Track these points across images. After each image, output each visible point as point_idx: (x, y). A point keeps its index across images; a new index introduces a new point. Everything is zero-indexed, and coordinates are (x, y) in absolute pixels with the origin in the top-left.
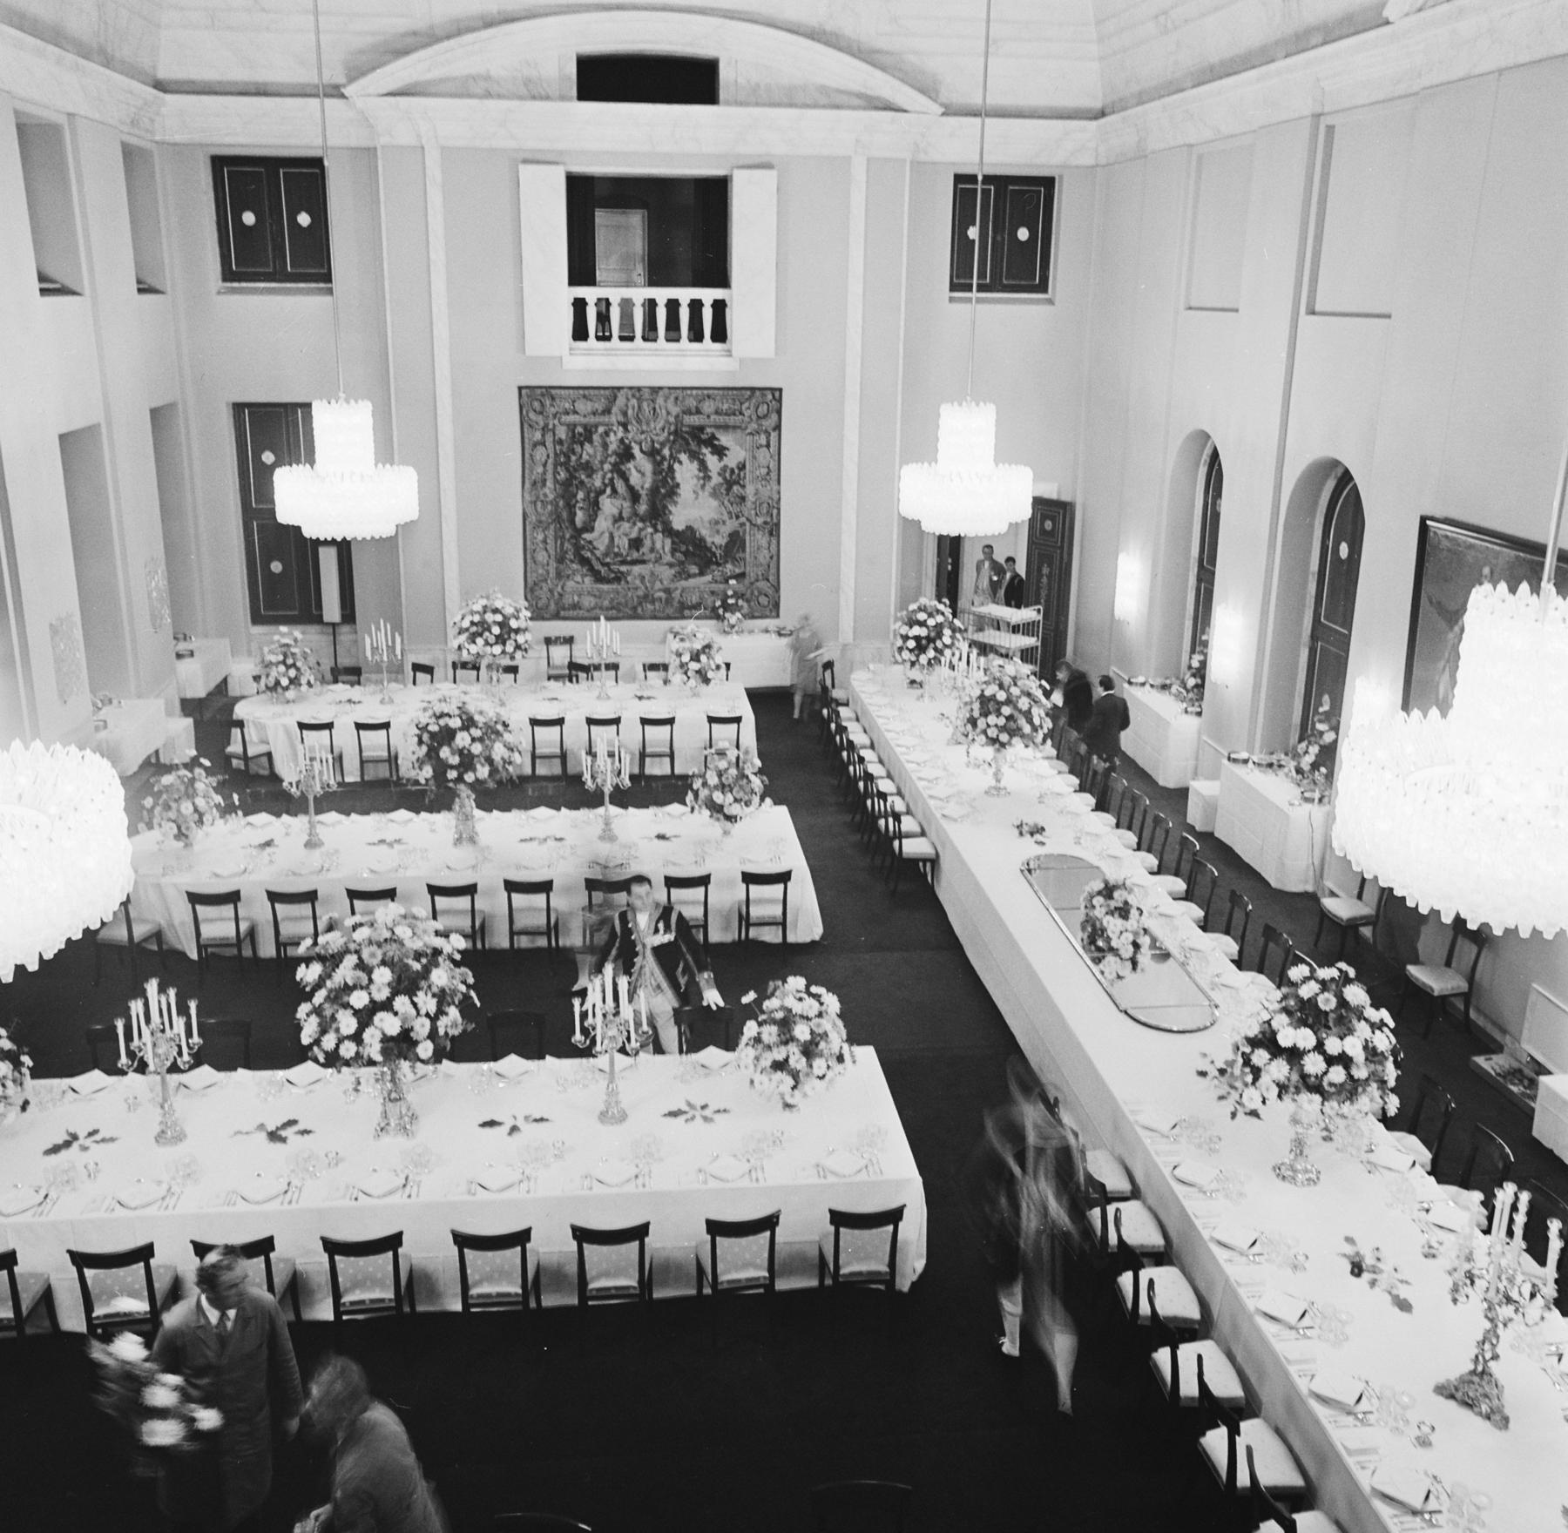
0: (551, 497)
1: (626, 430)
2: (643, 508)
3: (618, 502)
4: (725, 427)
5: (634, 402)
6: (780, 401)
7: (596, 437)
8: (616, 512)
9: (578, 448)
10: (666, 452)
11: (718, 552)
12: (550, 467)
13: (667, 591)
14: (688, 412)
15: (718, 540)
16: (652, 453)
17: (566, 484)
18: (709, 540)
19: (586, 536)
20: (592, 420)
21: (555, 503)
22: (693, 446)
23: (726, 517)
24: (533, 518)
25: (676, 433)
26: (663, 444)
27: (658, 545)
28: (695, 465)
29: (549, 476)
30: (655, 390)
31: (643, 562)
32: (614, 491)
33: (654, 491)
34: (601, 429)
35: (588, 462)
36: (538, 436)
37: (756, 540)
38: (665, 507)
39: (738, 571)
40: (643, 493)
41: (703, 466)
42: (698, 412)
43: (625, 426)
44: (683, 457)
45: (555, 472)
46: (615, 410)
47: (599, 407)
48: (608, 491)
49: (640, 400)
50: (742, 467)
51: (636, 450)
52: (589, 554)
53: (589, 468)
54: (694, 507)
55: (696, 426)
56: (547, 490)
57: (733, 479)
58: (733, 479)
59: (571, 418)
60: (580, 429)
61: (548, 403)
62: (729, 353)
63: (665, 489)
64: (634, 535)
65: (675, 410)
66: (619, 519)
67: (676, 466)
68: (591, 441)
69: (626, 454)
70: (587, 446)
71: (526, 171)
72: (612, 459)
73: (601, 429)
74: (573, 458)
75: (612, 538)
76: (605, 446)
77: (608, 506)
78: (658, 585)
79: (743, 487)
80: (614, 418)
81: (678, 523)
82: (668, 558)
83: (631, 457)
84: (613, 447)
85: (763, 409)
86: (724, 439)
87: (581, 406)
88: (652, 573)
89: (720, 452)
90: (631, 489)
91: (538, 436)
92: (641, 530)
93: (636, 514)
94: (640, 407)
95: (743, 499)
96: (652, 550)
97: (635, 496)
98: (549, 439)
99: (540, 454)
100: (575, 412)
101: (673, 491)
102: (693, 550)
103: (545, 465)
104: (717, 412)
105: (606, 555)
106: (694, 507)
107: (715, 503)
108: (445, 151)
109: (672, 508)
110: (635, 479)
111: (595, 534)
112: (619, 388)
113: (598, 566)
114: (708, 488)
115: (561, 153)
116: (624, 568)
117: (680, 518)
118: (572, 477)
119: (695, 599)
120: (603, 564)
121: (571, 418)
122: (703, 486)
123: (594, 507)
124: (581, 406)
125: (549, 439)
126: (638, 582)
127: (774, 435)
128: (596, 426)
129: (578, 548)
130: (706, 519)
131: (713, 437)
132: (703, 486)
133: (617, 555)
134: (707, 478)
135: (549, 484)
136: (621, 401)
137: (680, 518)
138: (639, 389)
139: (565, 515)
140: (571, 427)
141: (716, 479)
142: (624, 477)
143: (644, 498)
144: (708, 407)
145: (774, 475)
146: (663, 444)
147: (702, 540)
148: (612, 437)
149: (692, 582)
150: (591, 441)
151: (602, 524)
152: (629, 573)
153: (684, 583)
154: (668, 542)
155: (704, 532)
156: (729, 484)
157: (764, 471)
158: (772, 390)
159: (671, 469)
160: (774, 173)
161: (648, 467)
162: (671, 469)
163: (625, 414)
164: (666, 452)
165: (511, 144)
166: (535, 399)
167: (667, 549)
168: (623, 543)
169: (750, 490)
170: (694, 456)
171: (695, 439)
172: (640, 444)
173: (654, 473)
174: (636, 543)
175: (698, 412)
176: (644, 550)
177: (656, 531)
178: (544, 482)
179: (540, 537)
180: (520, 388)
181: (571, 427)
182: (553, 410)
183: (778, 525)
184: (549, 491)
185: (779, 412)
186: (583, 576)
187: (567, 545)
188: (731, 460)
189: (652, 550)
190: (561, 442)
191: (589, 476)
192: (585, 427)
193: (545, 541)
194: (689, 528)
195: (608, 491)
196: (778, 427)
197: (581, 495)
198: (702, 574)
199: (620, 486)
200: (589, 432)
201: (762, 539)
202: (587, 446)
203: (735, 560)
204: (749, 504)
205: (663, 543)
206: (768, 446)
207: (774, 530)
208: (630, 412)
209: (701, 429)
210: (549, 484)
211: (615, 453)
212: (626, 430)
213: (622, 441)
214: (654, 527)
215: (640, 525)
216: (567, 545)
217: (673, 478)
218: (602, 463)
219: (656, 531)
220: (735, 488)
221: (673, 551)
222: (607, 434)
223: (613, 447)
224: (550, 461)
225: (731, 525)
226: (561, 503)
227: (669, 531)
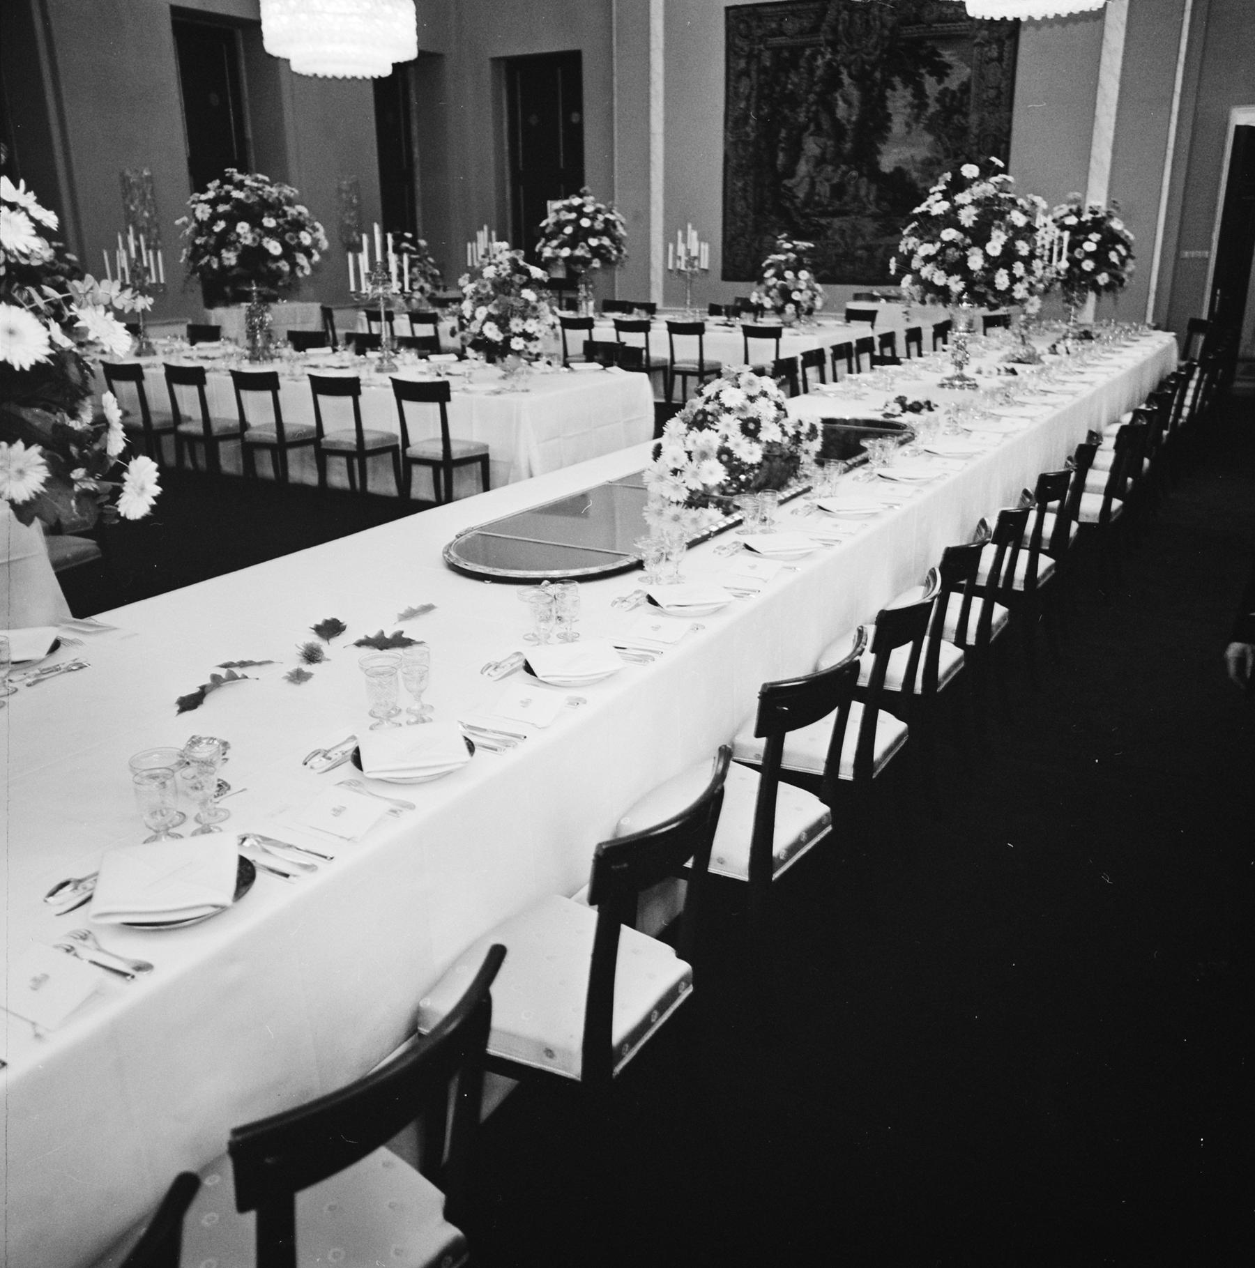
0: (753, 135)
1: (835, 52)
5: (845, 14)
7: (802, 63)
8: (817, 151)
12: (753, 100)
16: (861, 79)
19: (786, 182)
20: (799, 40)
23: (941, 157)
24: (733, 162)
26: (874, 66)
27: (863, 192)
31: (846, 213)
32: (819, 126)
33: (861, 124)
34: (808, 52)
35: (792, 92)
36: (742, 64)
41: (920, 93)
42: (918, 20)
43: (833, 44)
44: (897, 80)
45: (759, 108)
46: (824, 27)
48: (812, 127)
50: (965, 88)
53: (793, 101)
56: (748, 129)
57: (954, 104)
60: (786, 54)
61: (754, 24)
63: (874, 125)
66: (820, 161)
67: (889, 93)
69: (833, 82)
72: (817, 89)
73: (808, 52)
74: (778, 89)
76: (811, 71)
77: (812, 147)
79: (966, 115)
82: (872, 209)
83: (840, 84)
84: (819, 72)
86: (948, 56)
88: (854, 227)
90: (835, 122)
92: (845, 173)
94: (851, 21)
95: (964, 130)
97: (838, 131)
100: (782, 34)
105: (806, 203)
107: (929, 138)
109: (883, 148)
110: (841, 110)
111: (797, 179)
113: (797, 219)
114: (924, 120)
116: (823, 221)
125: (754, 67)
126: (837, 237)
127: (1008, 43)
128: (803, 48)
130: (918, 158)
132: (917, 119)
133: (819, 204)
140: (776, 51)
142: (831, 109)
146: (874, 66)
148: (820, 62)
150: (796, 67)
151: (803, 168)
154: (874, 187)
155: (915, 175)
157: (992, 93)
159: (883, 99)
161: (855, 94)
163: (834, 30)
164: (878, 75)
167: (872, 198)
168: (824, 189)
169: (974, 119)
172: (848, 66)
175: (918, 20)
176: (846, 198)
177: (861, 175)
179: (740, 184)
181: (776, 51)
182: (760, 32)
188: (953, 83)
189: (856, 198)
191: (793, 110)
193: (744, 190)
195: (812, 127)
197: (783, 134)
204: (972, 139)
205: (867, 190)
208: (840, 28)
213: (828, 65)
214: (858, 169)
215: (844, 167)
217: (885, 108)
218: (808, 92)
219: (861, 175)
222: (813, 57)
223: (819, 72)
224: (754, 93)
226: (763, 145)
227: (875, 174)
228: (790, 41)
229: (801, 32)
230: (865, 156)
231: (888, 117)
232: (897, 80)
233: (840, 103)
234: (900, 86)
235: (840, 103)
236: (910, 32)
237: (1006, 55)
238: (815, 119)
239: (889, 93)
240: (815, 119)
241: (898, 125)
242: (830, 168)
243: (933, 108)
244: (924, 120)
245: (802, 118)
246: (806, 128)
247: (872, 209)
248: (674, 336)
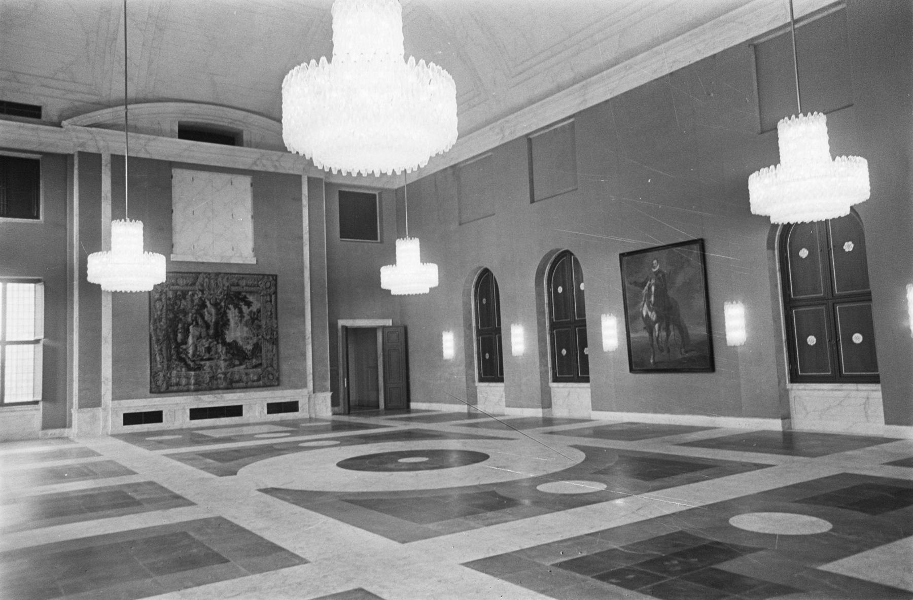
1: (203, 293)
2: (211, 332)
3: (199, 329)
4: (251, 293)
5: (206, 280)
6: (276, 280)
7: (188, 297)
8: (197, 333)
9: (178, 302)
10: (223, 304)
11: (249, 353)
12: (164, 311)
13: (225, 374)
14: (233, 285)
16: (216, 305)
19: (184, 347)
26: (221, 300)
27: (220, 350)
30: (218, 274)
32: (197, 323)
33: (217, 323)
37: (266, 347)
38: (222, 331)
40: (212, 324)
41: (241, 311)
42: (238, 285)
43: (202, 291)
44: (231, 306)
46: (197, 283)
47: (190, 281)
50: (259, 311)
51: (208, 303)
54: (236, 332)
57: (255, 317)
63: (222, 323)
65: (227, 284)
66: (199, 337)
68: (185, 298)
69: (203, 305)
70: (183, 301)
76: (192, 301)
78: (219, 371)
81: (228, 340)
83: (206, 306)
84: (196, 302)
86: (251, 298)
89: (249, 304)
90: (206, 322)
93: (208, 335)
95: (260, 327)
101: (226, 323)
102: (236, 352)
106: (236, 332)
107: (246, 329)
112: (200, 273)
114: (243, 322)
116: (202, 363)
117: (230, 337)
118: (175, 317)
119: (237, 377)
120: (193, 361)
121: (176, 287)
122: (241, 321)
123: (186, 332)
124: (180, 282)
125: (163, 297)
128: (188, 291)
129: (178, 353)
131: (245, 297)
132: (241, 321)
133: (199, 356)
137: (230, 337)
138: (209, 274)
139: (172, 336)
140: (175, 292)
141: (247, 317)
142: (203, 317)
145: (274, 315)
146: (221, 300)
147: (241, 347)
148: (196, 297)
149: (236, 369)
150: (185, 298)
152: (205, 365)
153: (231, 370)
155: (241, 343)
156: (253, 320)
158: (273, 276)
159: (225, 313)
161: (213, 311)
163: (202, 285)
164: (223, 304)
168: (202, 350)
169: (263, 322)
170: (236, 306)
171: (237, 298)
172: (210, 300)
173: (217, 314)
174: (209, 350)
175: (238, 285)
176: (212, 353)
181: (175, 292)
185: (276, 285)
186: (181, 367)
187: (173, 352)
188: (254, 308)
189: (217, 353)
190: (170, 299)
192: (182, 292)
194: (235, 341)
196: (275, 293)
197: (180, 326)
198: (241, 364)
202: (183, 301)
203: (257, 357)
206: (271, 301)
207: (275, 341)
209: (240, 293)
212: (203, 293)
213: (200, 298)
216: (173, 352)
221: (227, 353)
222: (193, 295)
223: (196, 302)
225: (255, 340)
227: (224, 343)
229: (187, 285)
231: (228, 320)
232: (231, 306)
234: (233, 309)
236: (233, 289)
238: (195, 320)
240: (195, 320)
244: (243, 322)
245: (189, 320)
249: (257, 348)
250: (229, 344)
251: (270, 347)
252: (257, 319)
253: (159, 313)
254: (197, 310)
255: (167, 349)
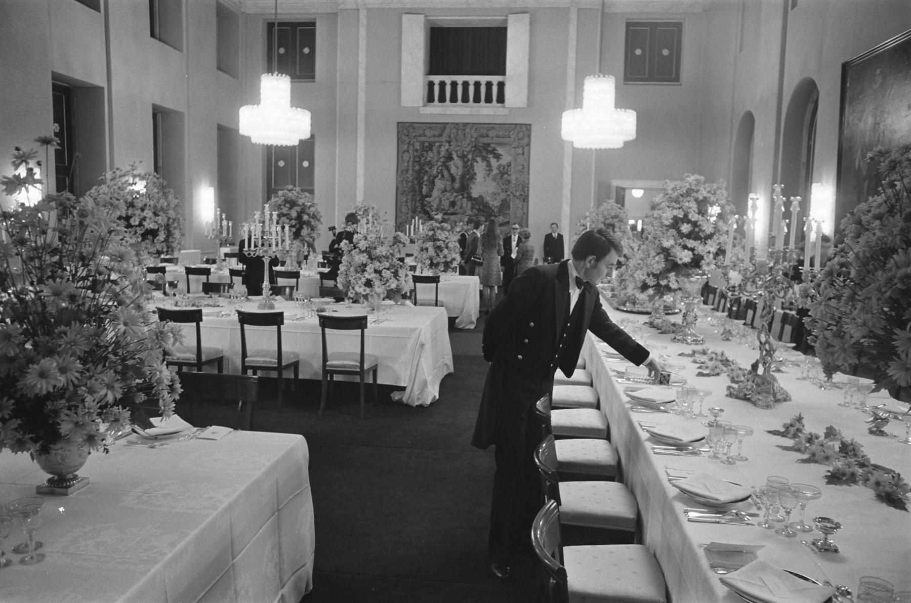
0: (411, 178)
1: (450, 145)
2: (457, 185)
3: (445, 182)
4: (501, 144)
5: (454, 131)
6: (530, 130)
7: (434, 148)
8: (443, 187)
9: (425, 154)
10: (470, 156)
11: (496, 210)
12: (411, 163)
15: (495, 203)
16: (463, 157)
17: (419, 172)
18: (491, 203)
20: (433, 139)
21: (412, 182)
22: (484, 154)
23: (500, 191)
24: (401, 189)
25: (475, 146)
26: (468, 153)
27: (464, 205)
28: (485, 163)
29: (410, 168)
31: (456, 214)
32: (443, 176)
33: (463, 177)
34: (437, 144)
36: (405, 147)
37: (515, 204)
39: (506, 220)
40: (457, 177)
41: (489, 165)
42: (487, 136)
43: (449, 142)
44: (479, 159)
45: (414, 166)
46: (445, 134)
47: (436, 133)
49: (457, 129)
50: (509, 165)
51: (455, 156)
52: (428, 209)
55: (484, 143)
57: (504, 172)
58: (504, 172)
59: (423, 139)
60: (426, 144)
62: (504, 107)
63: (468, 177)
64: (452, 200)
66: (445, 191)
67: (475, 164)
69: (449, 158)
70: (430, 153)
71: (405, 18)
72: (442, 160)
73: (437, 144)
75: (440, 201)
76: (439, 153)
77: (439, 184)
80: (444, 139)
81: (475, 194)
82: (469, 212)
84: (443, 154)
85: (521, 135)
86: (500, 151)
87: (429, 133)
89: (498, 157)
91: (405, 147)
93: (453, 188)
95: (509, 182)
96: (461, 207)
97: (453, 179)
98: (411, 148)
99: (406, 156)
101: (473, 177)
103: (408, 162)
104: (497, 136)
106: (483, 186)
107: (495, 184)
108: (369, 10)
110: (453, 170)
112: (447, 124)
115: (423, 9)
117: (476, 191)
121: (423, 139)
122: (489, 175)
123: (433, 183)
124: (429, 133)
125: (411, 148)
127: (526, 148)
128: (435, 143)
129: (423, 206)
130: (490, 192)
131: (495, 149)
134: (491, 170)
135: (410, 172)
136: (448, 130)
137: (476, 191)
138: (457, 124)
139: (417, 188)
140: (422, 143)
141: (495, 171)
143: (458, 180)
144: (492, 133)
145: (526, 169)
146: (468, 153)
147: (487, 203)
148: (443, 149)
150: (431, 150)
151: (436, 193)
154: (470, 203)
155: (488, 199)
156: (502, 174)
157: (521, 167)
160: (528, 15)
161: (460, 163)
162: (472, 164)
163: (450, 137)
164: (470, 156)
165: (400, 6)
166: (406, 130)
167: (469, 207)
169: (513, 178)
170: (484, 159)
171: (485, 150)
172: (456, 152)
173: (464, 167)
174: (453, 204)
178: (407, 170)
179: (405, 199)
180: (398, 123)
181: (422, 143)
182: (414, 134)
183: (528, 196)
184: (410, 175)
185: (529, 136)
187: (418, 204)
188: (504, 161)
189: (461, 207)
190: (417, 151)
192: (429, 143)
193: (406, 202)
194: (481, 196)
195: (440, 176)
196: (529, 145)
197: (426, 178)
199: (446, 173)
200: (431, 145)
201: (519, 203)
202: (430, 153)
204: (512, 185)
206: (523, 154)
207: (525, 199)
209: (488, 145)
210: (410, 172)
211: (444, 157)
212: (450, 145)
213: (447, 150)
214: (462, 195)
218: (437, 161)
220: (505, 176)
221: (472, 208)
222: (440, 146)
223: (443, 154)
225: (503, 196)
226: (416, 182)
227: (470, 198)
228: (429, 140)
229: (434, 136)
230: (464, 189)
232: (479, 159)
233: (453, 166)
235: (453, 166)
237: (526, 152)
239: (475, 164)
241: (479, 177)
242: (448, 194)
243: (495, 171)
245: (435, 172)
246: (437, 176)
247: (469, 212)
248: (246, 326)
249: (505, 205)
250: (475, 199)
251: (520, 206)
252: (506, 173)
253: (406, 164)
254: (444, 163)
255: (412, 200)
